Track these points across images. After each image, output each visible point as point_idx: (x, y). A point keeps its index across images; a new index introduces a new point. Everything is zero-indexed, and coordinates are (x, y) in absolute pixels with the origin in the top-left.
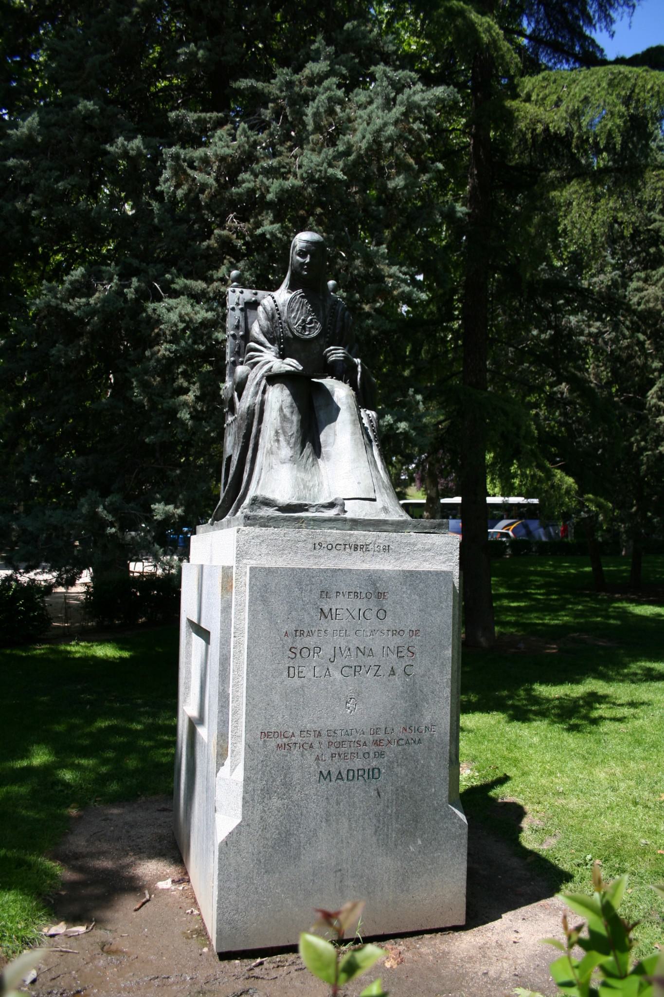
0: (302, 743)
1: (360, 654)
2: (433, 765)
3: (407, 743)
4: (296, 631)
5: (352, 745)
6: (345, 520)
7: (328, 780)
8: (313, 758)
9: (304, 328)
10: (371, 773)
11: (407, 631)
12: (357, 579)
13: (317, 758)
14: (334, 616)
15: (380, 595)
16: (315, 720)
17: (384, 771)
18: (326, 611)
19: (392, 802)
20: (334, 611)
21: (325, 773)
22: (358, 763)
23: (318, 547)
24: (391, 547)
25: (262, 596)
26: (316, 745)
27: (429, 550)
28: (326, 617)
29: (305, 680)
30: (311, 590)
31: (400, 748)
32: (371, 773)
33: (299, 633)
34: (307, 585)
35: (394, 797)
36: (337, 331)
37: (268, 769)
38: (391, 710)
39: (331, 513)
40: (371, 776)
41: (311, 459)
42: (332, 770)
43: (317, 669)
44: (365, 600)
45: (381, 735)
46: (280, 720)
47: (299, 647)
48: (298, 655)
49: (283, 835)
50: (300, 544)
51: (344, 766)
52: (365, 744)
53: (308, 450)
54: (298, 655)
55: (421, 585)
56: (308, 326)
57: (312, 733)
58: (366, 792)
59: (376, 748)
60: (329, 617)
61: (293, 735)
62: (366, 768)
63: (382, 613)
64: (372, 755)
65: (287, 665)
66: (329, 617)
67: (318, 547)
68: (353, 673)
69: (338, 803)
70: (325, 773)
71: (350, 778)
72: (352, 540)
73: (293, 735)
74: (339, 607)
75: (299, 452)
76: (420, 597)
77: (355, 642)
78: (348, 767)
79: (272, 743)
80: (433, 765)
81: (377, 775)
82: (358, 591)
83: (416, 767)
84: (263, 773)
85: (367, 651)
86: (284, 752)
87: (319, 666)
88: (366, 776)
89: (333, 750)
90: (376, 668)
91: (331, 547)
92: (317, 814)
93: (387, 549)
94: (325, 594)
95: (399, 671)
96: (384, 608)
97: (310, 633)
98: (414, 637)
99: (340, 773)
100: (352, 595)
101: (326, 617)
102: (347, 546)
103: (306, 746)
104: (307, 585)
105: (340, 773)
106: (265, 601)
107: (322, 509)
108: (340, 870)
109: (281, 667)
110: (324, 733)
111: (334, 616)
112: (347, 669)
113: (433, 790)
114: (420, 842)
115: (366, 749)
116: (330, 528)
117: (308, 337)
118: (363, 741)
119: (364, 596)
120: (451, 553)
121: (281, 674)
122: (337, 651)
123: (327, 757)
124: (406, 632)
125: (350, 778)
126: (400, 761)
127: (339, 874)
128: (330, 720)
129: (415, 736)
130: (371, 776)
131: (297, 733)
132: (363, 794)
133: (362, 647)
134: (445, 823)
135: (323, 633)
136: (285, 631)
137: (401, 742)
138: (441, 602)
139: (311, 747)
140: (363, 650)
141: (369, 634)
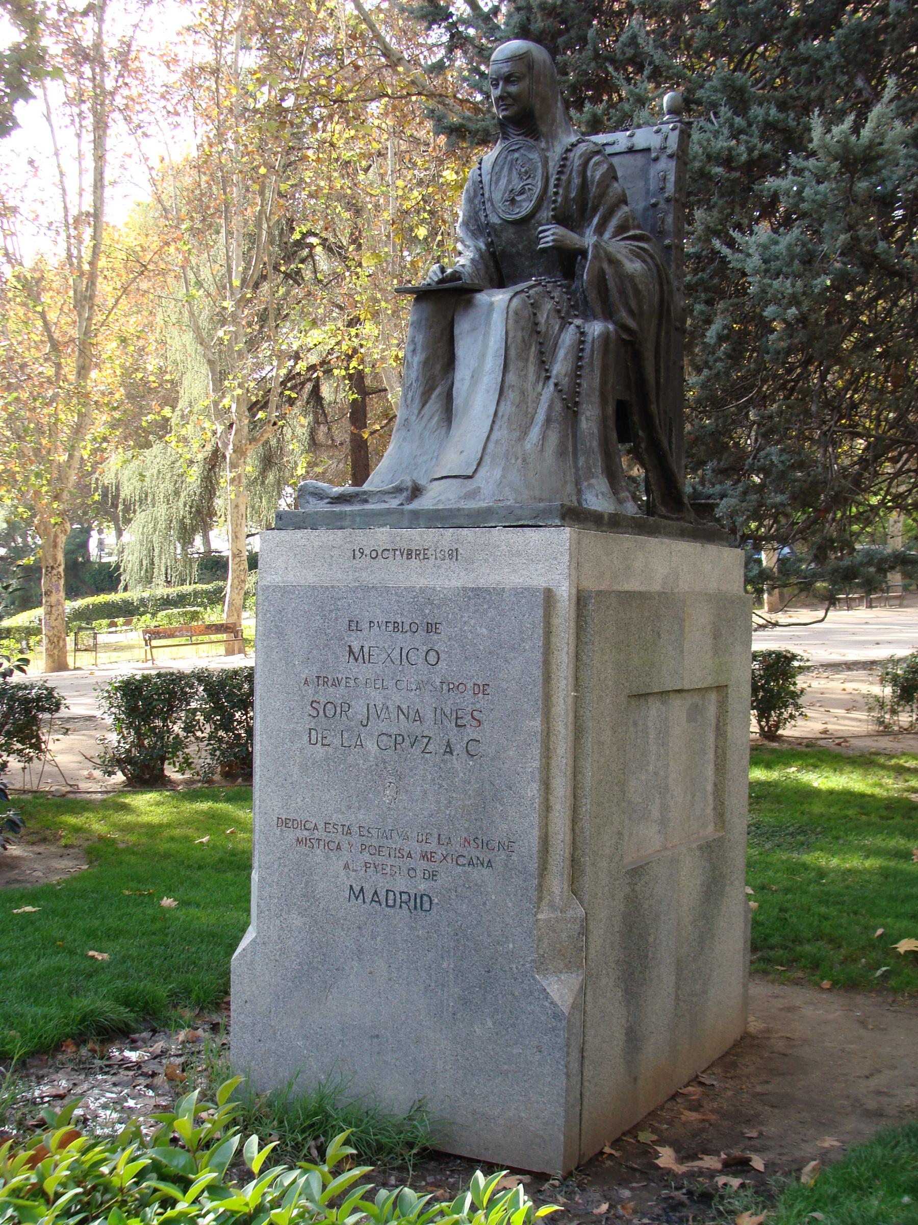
0: (327, 839)
1: (402, 716)
2: (510, 905)
3: (471, 863)
4: (318, 677)
5: (392, 853)
6: (402, 513)
7: (360, 900)
8: (341, 864)
9: (513, 201)
10: (418, 901)
11: (470, 685)
12: (398, 602)
13: (346, 866)
14: (366, 657)
15: (431, 628)
16: (343, 809)
17: (436, 901)
18: (356, 650)
19: (449, 952)
20: (366, 650)
21: (357, 889)
22: (401, 884)
23: (358, 554)
24: (460, 551)
25: (276, 626)
26: (345, 846)
27: (519, 554)
28: (356, 660)
29: (330, 750)
30: (336, 619)
31: (460, 869)
32: (418, 901)
33: (321, 680)
34: (331, 611)
35: (452, 944)
36: (573, 195)
37: (286, 870)
38: (447, 807)
39: (394, 503)
40: (418, 905)
41: (436, 419)
42: (366, 887)
43: (346, 735)
44: (409, 633)
45: (433, 846)
46: (300, 804)
47: (323, 700)
48: (321, 713)
49: (306, 967)
50: (336, 552)
51: (382, 884)
52: (410, 855)
53: (434, 404)
54: (321, 713)
55: (492, 613)
56: (518, 198)
57: (340, 829)
58: (411, 928)
59: (424, 864)
60: (360, 660)
61: (316, 828)
62: (412, 892)
63: (432, 656)
64: (420, 874)
65: (308, 727)
66: (360, 660)
67: (358, 554)
68: (392, 744)
69: (374, 938)
70: (357, 889)
71: (391, 902)
72: (404, 545)
73: (316, 828)
74: (373, 644)
75: (416, 412)
76: (491, 631)
77: (396, 698)
78: (388, 887)
79: (291, 835)
80: (510, 905)
81: (426, 906)
82: (399, 621)
83: (485, 904)
84: (281, 874)
85: (412, 714)
86: (303, 849)
87: (348, 730)
88: (412, 903)
89: (366, 857)
90: (426, 740)
91: (375, 555)
92: (347, 947)
93: (454, 554)
94: (353, 625)
95: (458, 748)
96: (436, 648)
97: (336, 683)
98: (481, 695)
99: (376, 893)
100: (391, 628)
101: (356, 660)
102: (398, 553)
103: (332, 845)
104: (331, 611)
105: (376, 893)
106: (281, 635)
107: (386, 498)
108: (377, 1036)
109: (299, 728)
110: (355, 829)
111: (366, 657)
112: (384, 738)
113: (511, 946)
114: (490, 1024)
115: (411, 863)
116: (382, 526)
117: (518, 217)
118: (407, 849)
119: (407, 628)
120: (556, 559)
121: (301, 738)
122: (372, 710)
123: (359, 865)
124: (468, 686)
125: (391, 902)
126: (459, 890)
127: (375, 1040)
128: (362, 811)
129: (485, 856)
130: (418, 905)
131: (321, 826)
132: (407, 930)
133: (404, 707)
134: (530, 1003)
135: (352, 682)
136: (304, 676)
137: (461, 861)
138: (523, 640)
139: (339, 848)
140: (406, 711)
141: (414, 687)
